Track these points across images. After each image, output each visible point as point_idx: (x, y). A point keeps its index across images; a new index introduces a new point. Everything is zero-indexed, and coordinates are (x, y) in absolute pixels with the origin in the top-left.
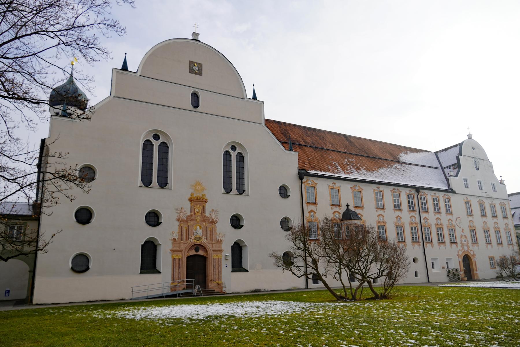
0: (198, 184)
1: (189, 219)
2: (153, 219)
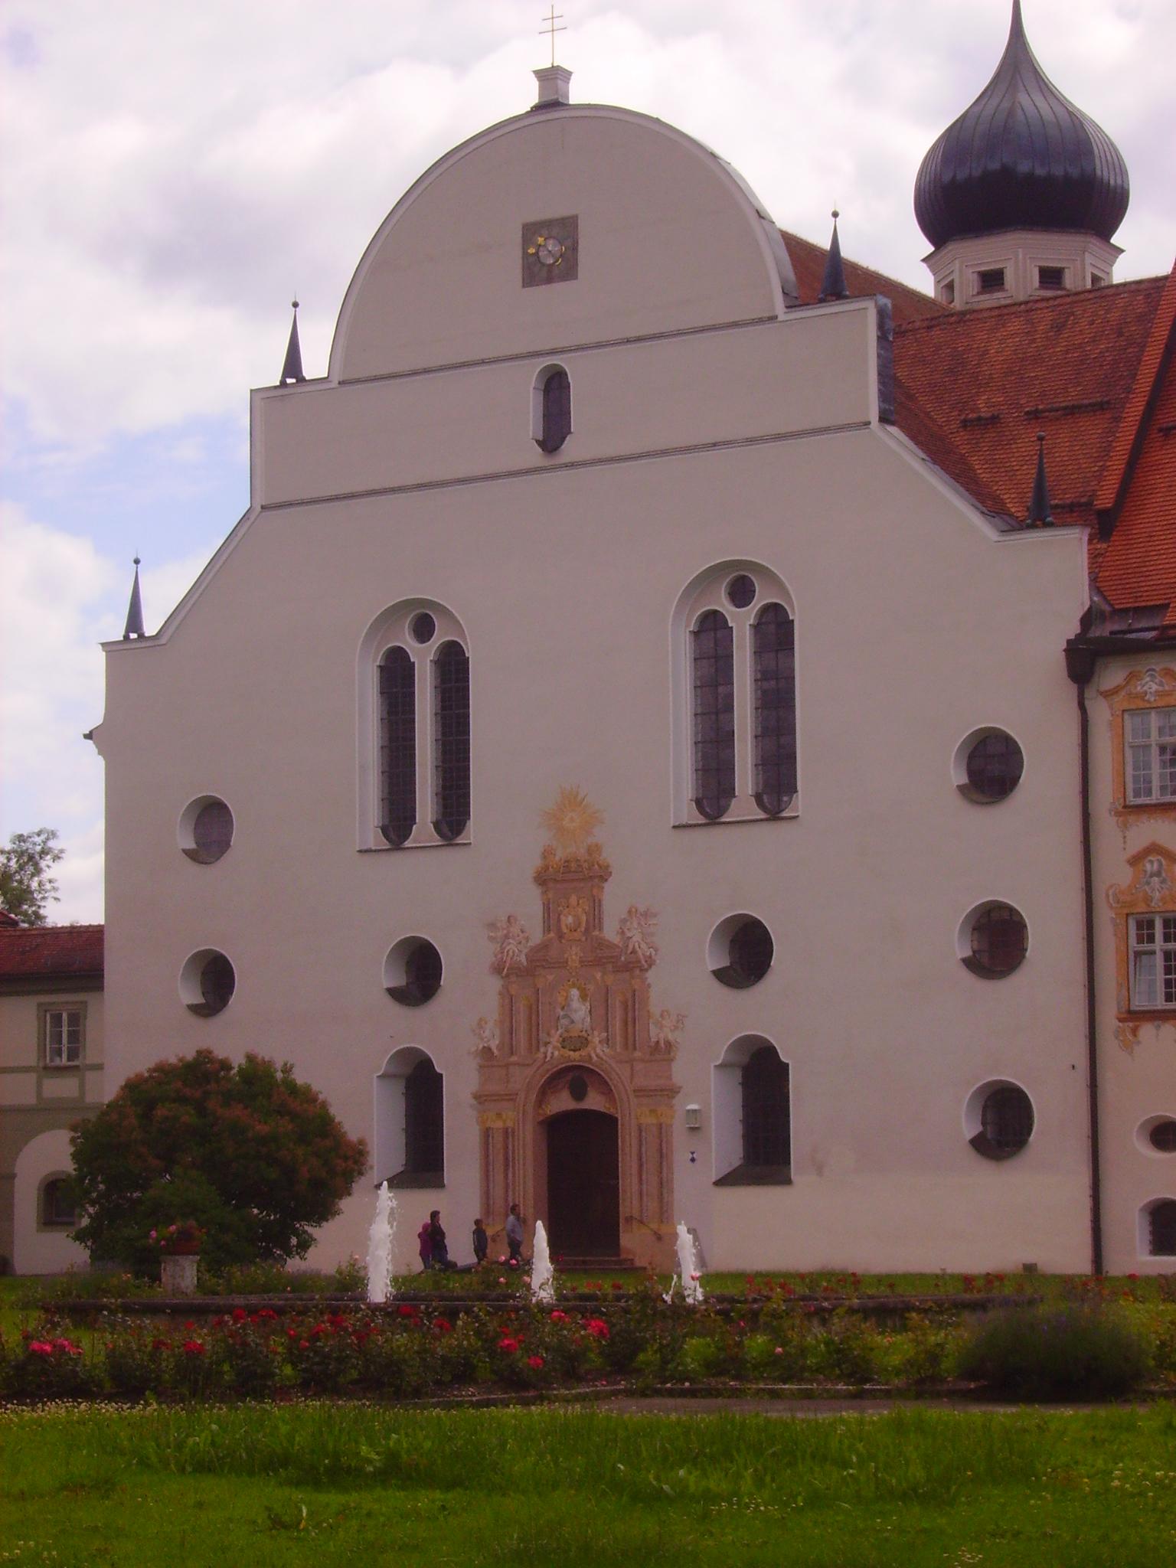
0: (571, 801)
1: (540, 960)
2: (420, 971)
